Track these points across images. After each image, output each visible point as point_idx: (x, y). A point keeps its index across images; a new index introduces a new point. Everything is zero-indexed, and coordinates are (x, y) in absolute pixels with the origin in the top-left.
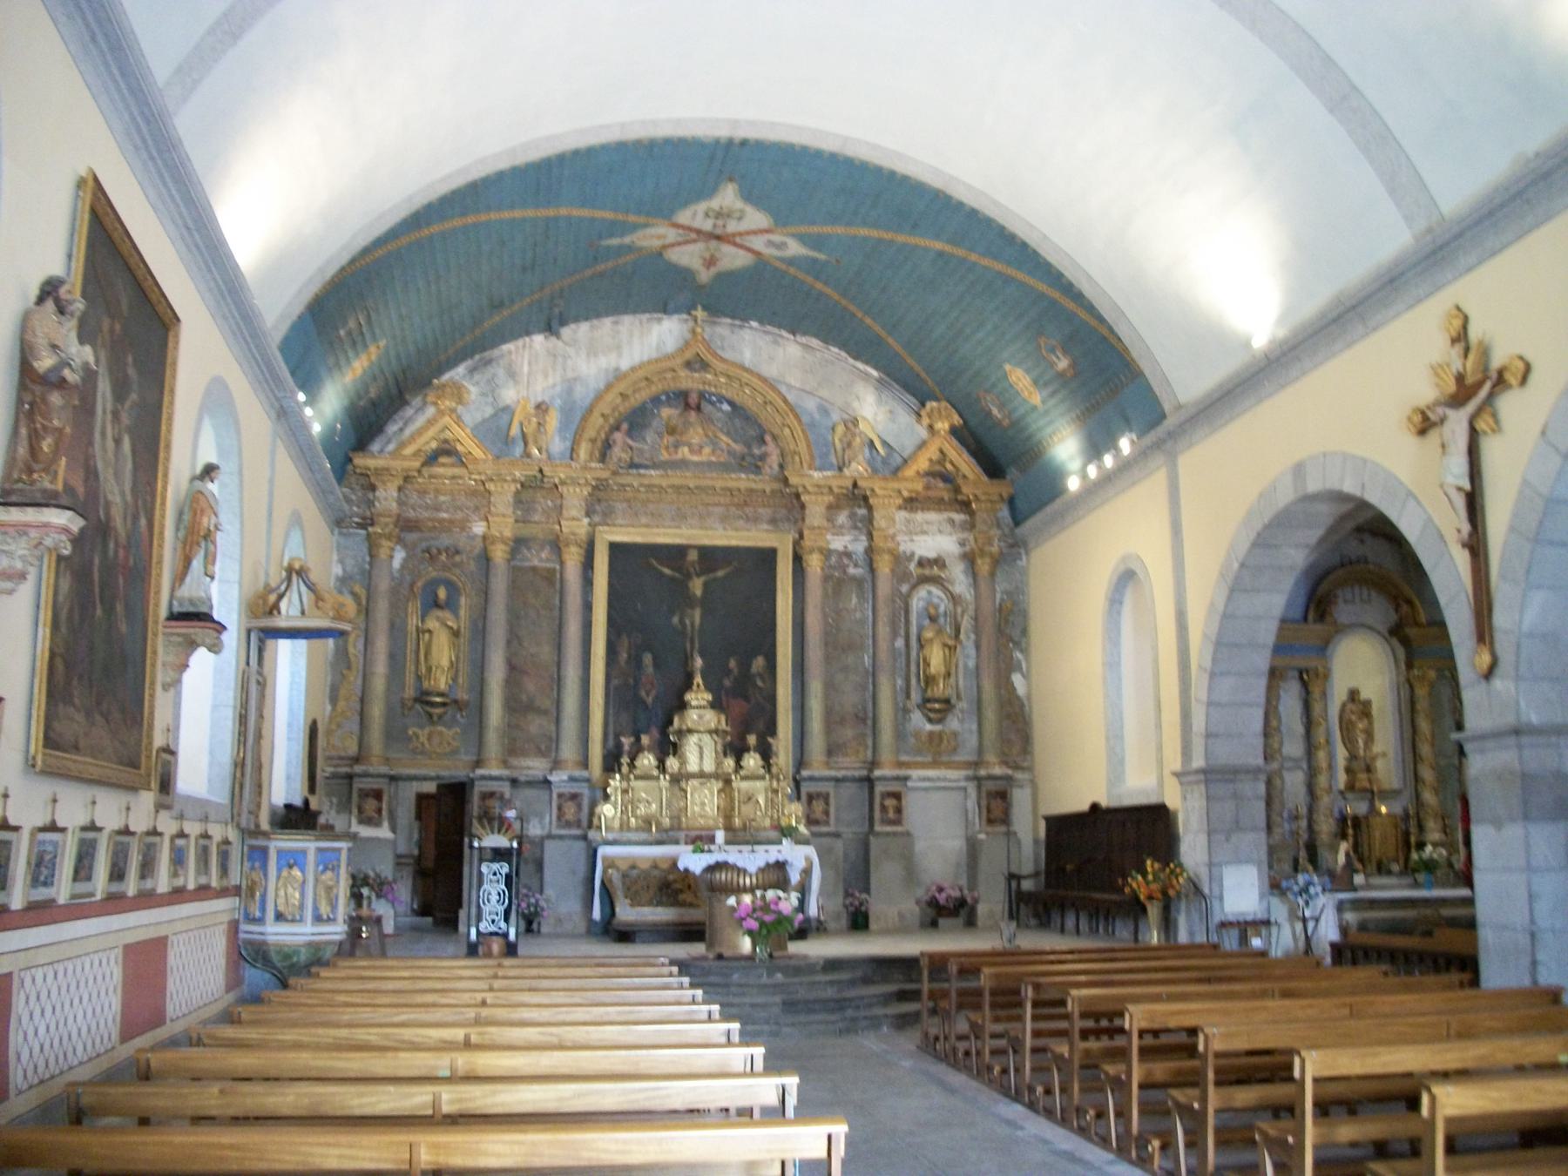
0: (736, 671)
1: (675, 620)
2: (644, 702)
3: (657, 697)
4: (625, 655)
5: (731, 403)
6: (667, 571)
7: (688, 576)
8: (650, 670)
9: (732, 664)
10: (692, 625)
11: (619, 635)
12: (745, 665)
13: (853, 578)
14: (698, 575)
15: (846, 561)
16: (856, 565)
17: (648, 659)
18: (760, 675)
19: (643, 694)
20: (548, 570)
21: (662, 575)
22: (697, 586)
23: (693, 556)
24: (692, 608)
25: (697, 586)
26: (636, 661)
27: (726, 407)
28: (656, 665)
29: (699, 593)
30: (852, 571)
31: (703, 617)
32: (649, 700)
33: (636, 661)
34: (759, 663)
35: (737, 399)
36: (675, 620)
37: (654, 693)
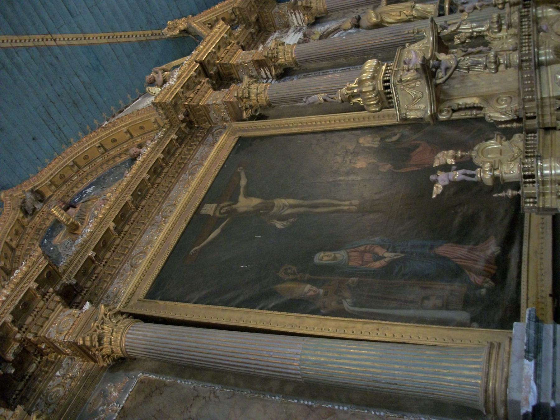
1: (279, 225)
2: (392, 264)
3: (383, 246)
4: (308, 287)
5: (89, 187)
8: (341, 255)
10: (291, 206)
11: (273, 293)
14: (236, 201)
17: (323, 258)
18: (382, 139)
19: (378, 264)
20: (138, 391)
25: (245, 203)
26: (319, 274)
28: (335, 248)
29: (256, 201)
32: (389, 256)
33: (319, 274)
35: (91, 179)
36: (279, 225)
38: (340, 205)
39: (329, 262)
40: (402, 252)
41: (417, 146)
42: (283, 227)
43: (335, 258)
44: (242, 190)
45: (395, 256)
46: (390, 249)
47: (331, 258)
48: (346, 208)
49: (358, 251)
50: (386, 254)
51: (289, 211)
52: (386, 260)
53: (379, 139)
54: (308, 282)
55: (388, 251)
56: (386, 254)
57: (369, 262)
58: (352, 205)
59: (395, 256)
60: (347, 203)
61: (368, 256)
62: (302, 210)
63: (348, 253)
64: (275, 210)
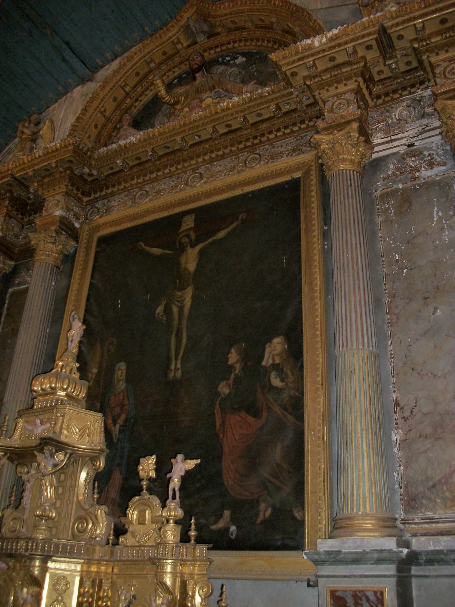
0: (238, 366)
1: (160, 310)
3: (126, 420)
4: (95, 370)
5: (243, 55)
6: (156, 251)
7: (182, 250)
8: (122, 386)
9: (233, 357)
10: (181, 309)
12: (253, 357)
13: (429, 185)
14: (193, 246)
15: (412, 162)
16: (431, 165)
18: (275, 367)
21: (149, 255)
22: (190, 261)
23: (189, 222)
24: (183, 288)
27: (241, 60)
29: (192, 267)
30: (425, 173)
31: (194, 298)
34: (275, 348)
36: (160, 310)
37: (123, 417)
38: (176, 359)
39: (116, 377)
40: (118, 440)
41: (256, 415)
42: (156, 315)
43: (119, 381)
44: (211, 240)
45: (116, 435)
46: (122, 428)
47: (120, 377)
48: (173, 367)
49: (123, 399)
50: (118, 426)
51: (175, 309)
52: (113, 428)
53: (277, 361)
54: (100, 370)
55: (120, 426)
56: (118, 426)
57: (111, 414)
58: (175, 372)
59: (116, 435)
60: (179, 366)
61: (117, 410)
62: (175, 322)
63: (123, 391)
64: (179, 294)
